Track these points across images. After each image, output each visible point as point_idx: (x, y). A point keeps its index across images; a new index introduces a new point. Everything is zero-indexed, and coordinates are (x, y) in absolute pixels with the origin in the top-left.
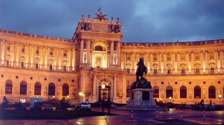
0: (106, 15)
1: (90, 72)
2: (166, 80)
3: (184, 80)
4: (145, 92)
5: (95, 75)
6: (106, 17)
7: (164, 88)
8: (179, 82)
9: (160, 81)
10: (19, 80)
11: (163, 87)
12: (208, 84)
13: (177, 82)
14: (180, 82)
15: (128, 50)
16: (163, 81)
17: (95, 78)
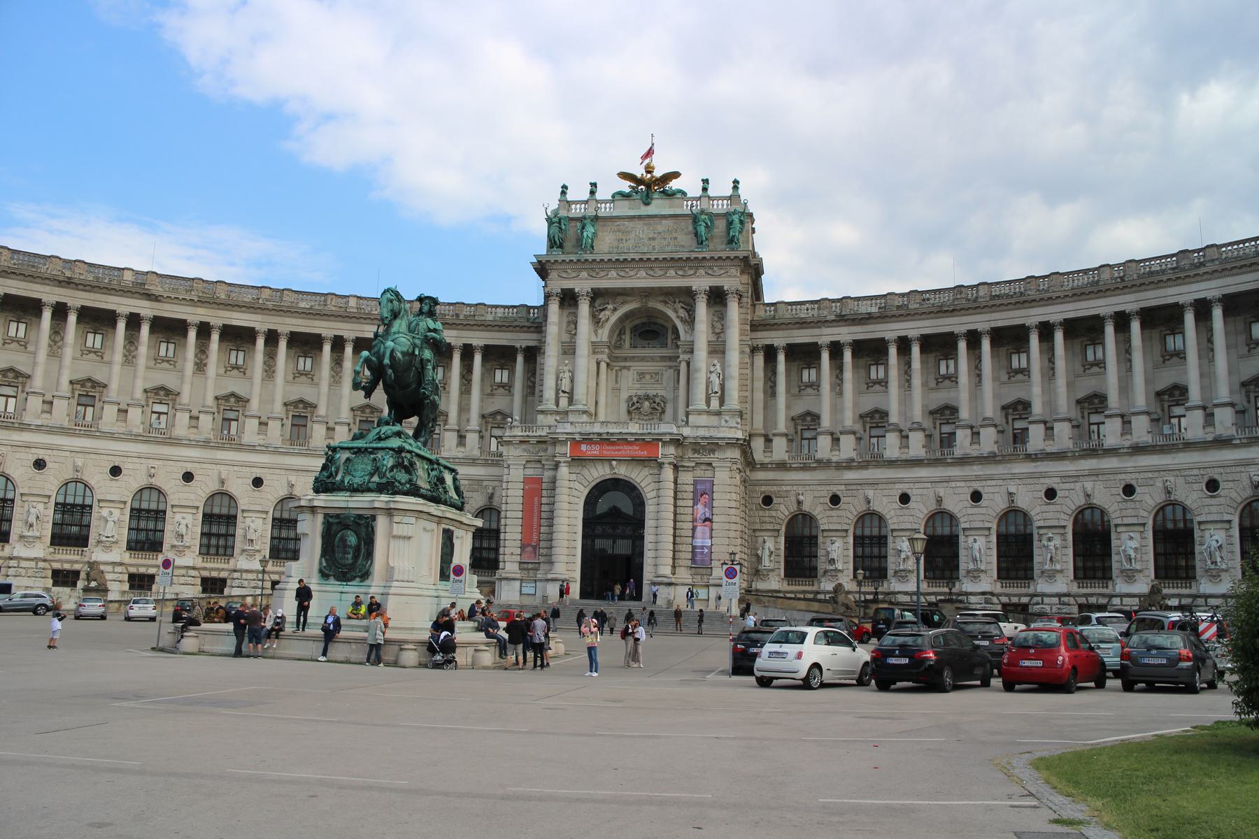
0: (676, 175)
1: (546, 450)
2: (993, 483)
3: (1095, 474)
4: (338, 516)
5: (562, 460)
6: (674, 185)
7: (987, 525)
8: (1067, 486)
9: (962, 484)
10: (270, 497)
11: (982, 517)
12: (1234, 495)
13: (1055, 486)
14: (1072, 486)
15: (796, 332)
16: (977, 486)
17: (564, 470)
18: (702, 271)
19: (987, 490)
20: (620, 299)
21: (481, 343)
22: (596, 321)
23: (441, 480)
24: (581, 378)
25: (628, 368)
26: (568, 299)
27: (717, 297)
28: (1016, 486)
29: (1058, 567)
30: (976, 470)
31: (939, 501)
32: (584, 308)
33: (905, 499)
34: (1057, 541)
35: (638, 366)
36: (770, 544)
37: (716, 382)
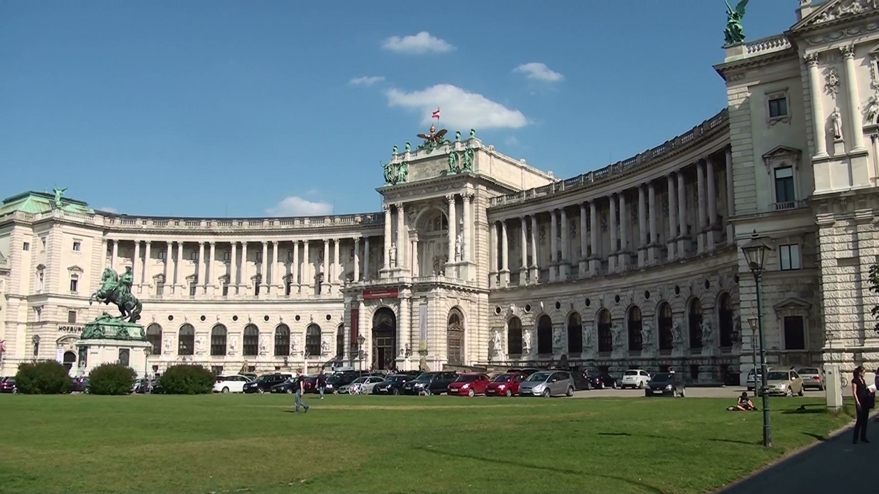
3: (634, 286)
16: (587, 295)
17: (362, 305)
18: (450, 187)
19: (593, 298)
20: (420, 206)
21: (367, 236)
22: (408, 220)
23: (126, 332)
24: (401, 251)
25: (433, 242)
26: (394, 210)
27: (459, 200)
28: (602, 295)
29: (620, 343)
30: (587, 287)
31: (572, 305)
32: (401, 214)
33: (558, 305)
34: (620, 326)
35: (437, 240)
36: (498, 336)
37: (459, 247)
